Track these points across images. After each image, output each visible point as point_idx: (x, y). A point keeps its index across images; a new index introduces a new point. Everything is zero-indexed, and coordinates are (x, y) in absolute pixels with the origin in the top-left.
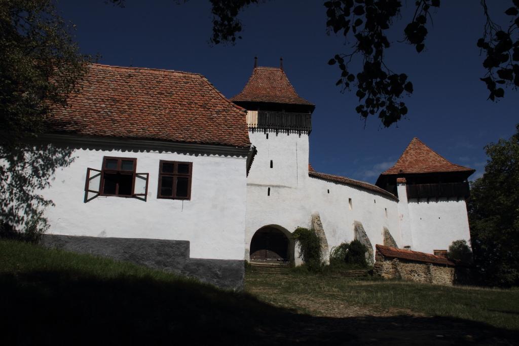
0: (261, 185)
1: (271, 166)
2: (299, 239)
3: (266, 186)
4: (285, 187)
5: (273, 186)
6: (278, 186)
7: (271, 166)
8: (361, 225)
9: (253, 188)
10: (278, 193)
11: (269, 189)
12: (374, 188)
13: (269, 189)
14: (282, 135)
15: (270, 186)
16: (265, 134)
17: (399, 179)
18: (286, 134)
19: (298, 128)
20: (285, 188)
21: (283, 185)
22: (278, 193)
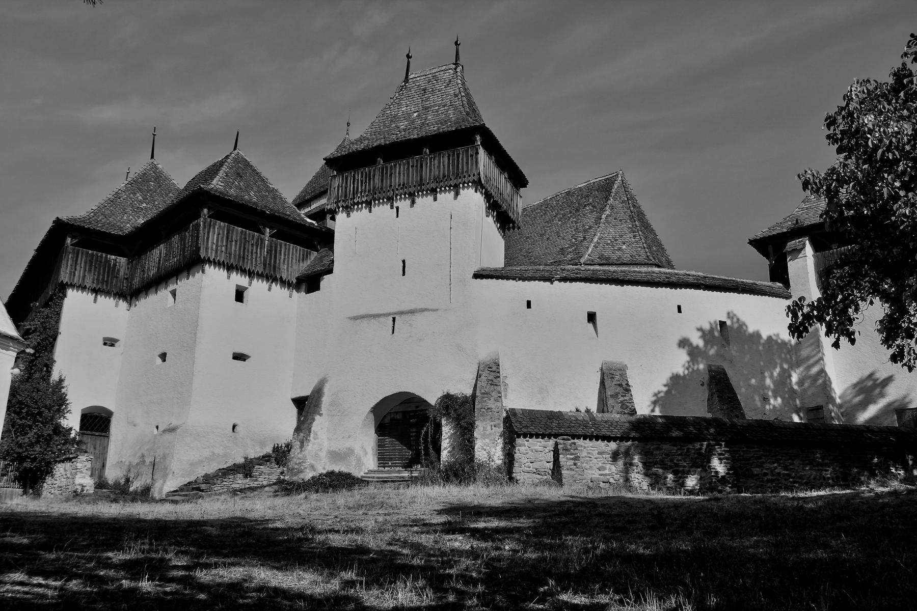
0: (379, 316)
1: (404, 274)
2: (447, 415)
3: (389, 314)
4: (423, 310)
5: (401, 313)
6: (412, 312)
7: (404, 274)
8: (622, 370)
9: (365, 322)
10: (411, 325)
11: (394, 319)
12: (663, 277)
13: (394, 319)
14: (424, 202)
15: (395, 313)
16: (392, 207)
17: (791, 244)
18: (430, 198)
19: (453, 183)
20: (426, 313)
21: (423, 306)
22: (411, 325)
